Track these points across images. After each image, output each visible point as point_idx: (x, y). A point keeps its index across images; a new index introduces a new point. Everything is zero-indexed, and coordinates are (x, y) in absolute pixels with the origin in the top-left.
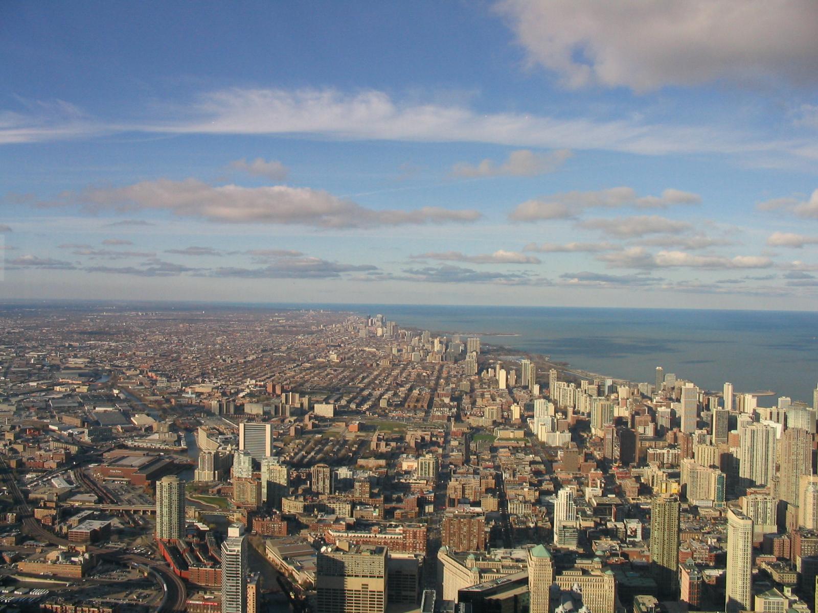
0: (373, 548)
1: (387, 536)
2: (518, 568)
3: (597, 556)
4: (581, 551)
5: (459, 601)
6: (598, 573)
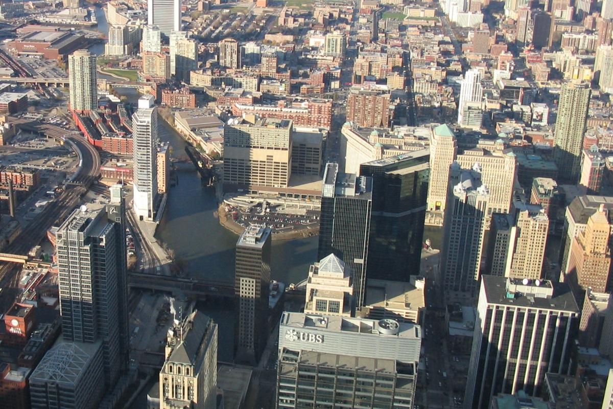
1: (293, 110)
2: (421, 145)
3: (500, 138)
4: (484, 132)
5: (360, 175)
6: (500, 154)
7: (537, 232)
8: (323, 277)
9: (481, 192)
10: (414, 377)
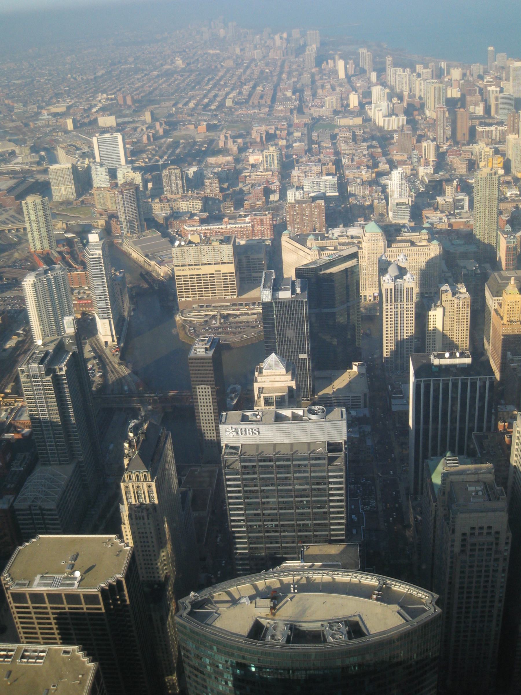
0: (221, 238)
1: (237, 226)
3: (424, 228)
4: (412, 224)
6: (425, 243)
7: (461, 309)
8: (268, 376)
9: (407, 280)
10: (342, 454)
